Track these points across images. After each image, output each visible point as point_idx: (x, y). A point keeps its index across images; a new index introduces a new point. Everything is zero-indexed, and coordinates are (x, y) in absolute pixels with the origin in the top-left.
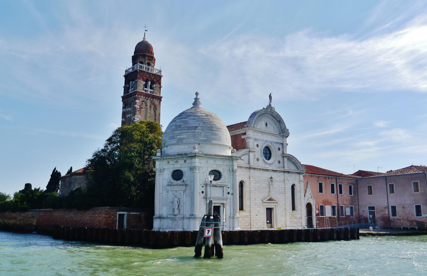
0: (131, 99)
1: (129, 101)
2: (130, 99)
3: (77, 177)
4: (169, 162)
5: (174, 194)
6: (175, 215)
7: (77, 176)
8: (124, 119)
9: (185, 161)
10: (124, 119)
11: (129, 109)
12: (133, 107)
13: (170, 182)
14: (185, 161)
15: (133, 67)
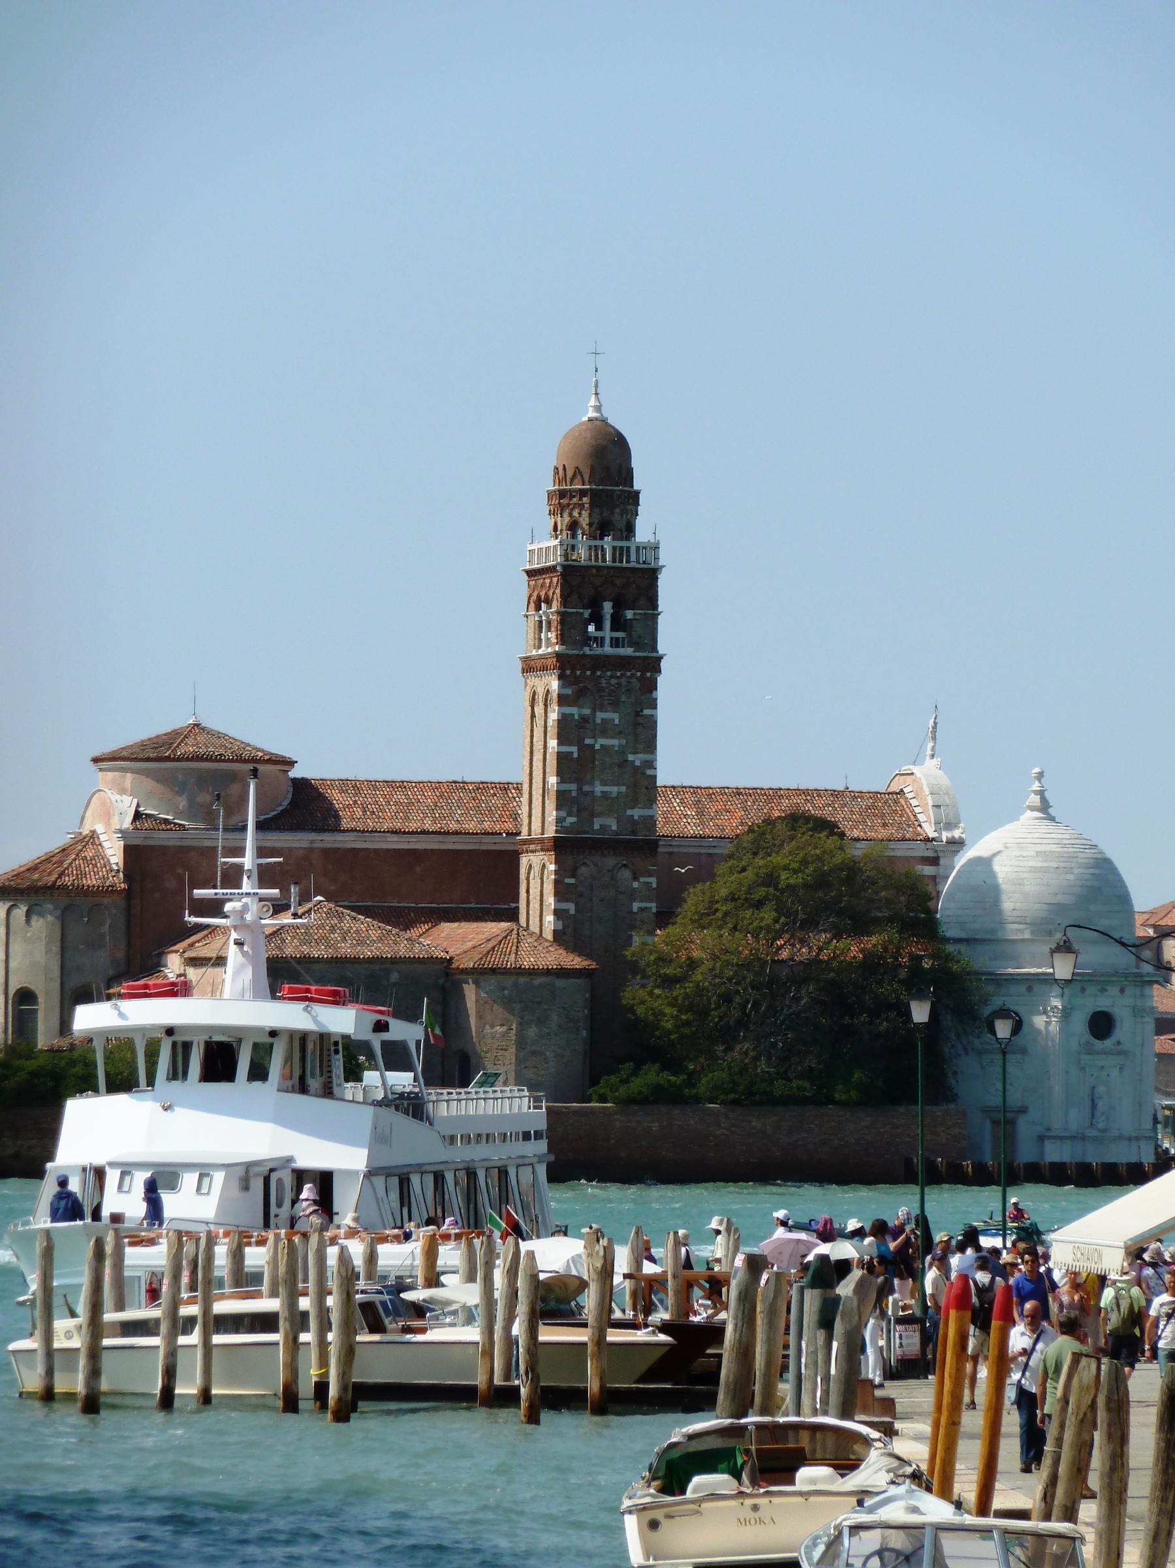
0: (623, 681)
1: (603, 681)
2: (611, 677)
3: (560, 983)
4: (1083, 990)
5: (1095, 1074)
6: (1104, 1131)
7: (558, 977)
8: (574, 749)
9: (1122, 990)
10: (574, 749)
11: (615, 717)
12: (638, 714)
13: (1087, 1043)
14: (1122, 990)
15: (621, 548)
